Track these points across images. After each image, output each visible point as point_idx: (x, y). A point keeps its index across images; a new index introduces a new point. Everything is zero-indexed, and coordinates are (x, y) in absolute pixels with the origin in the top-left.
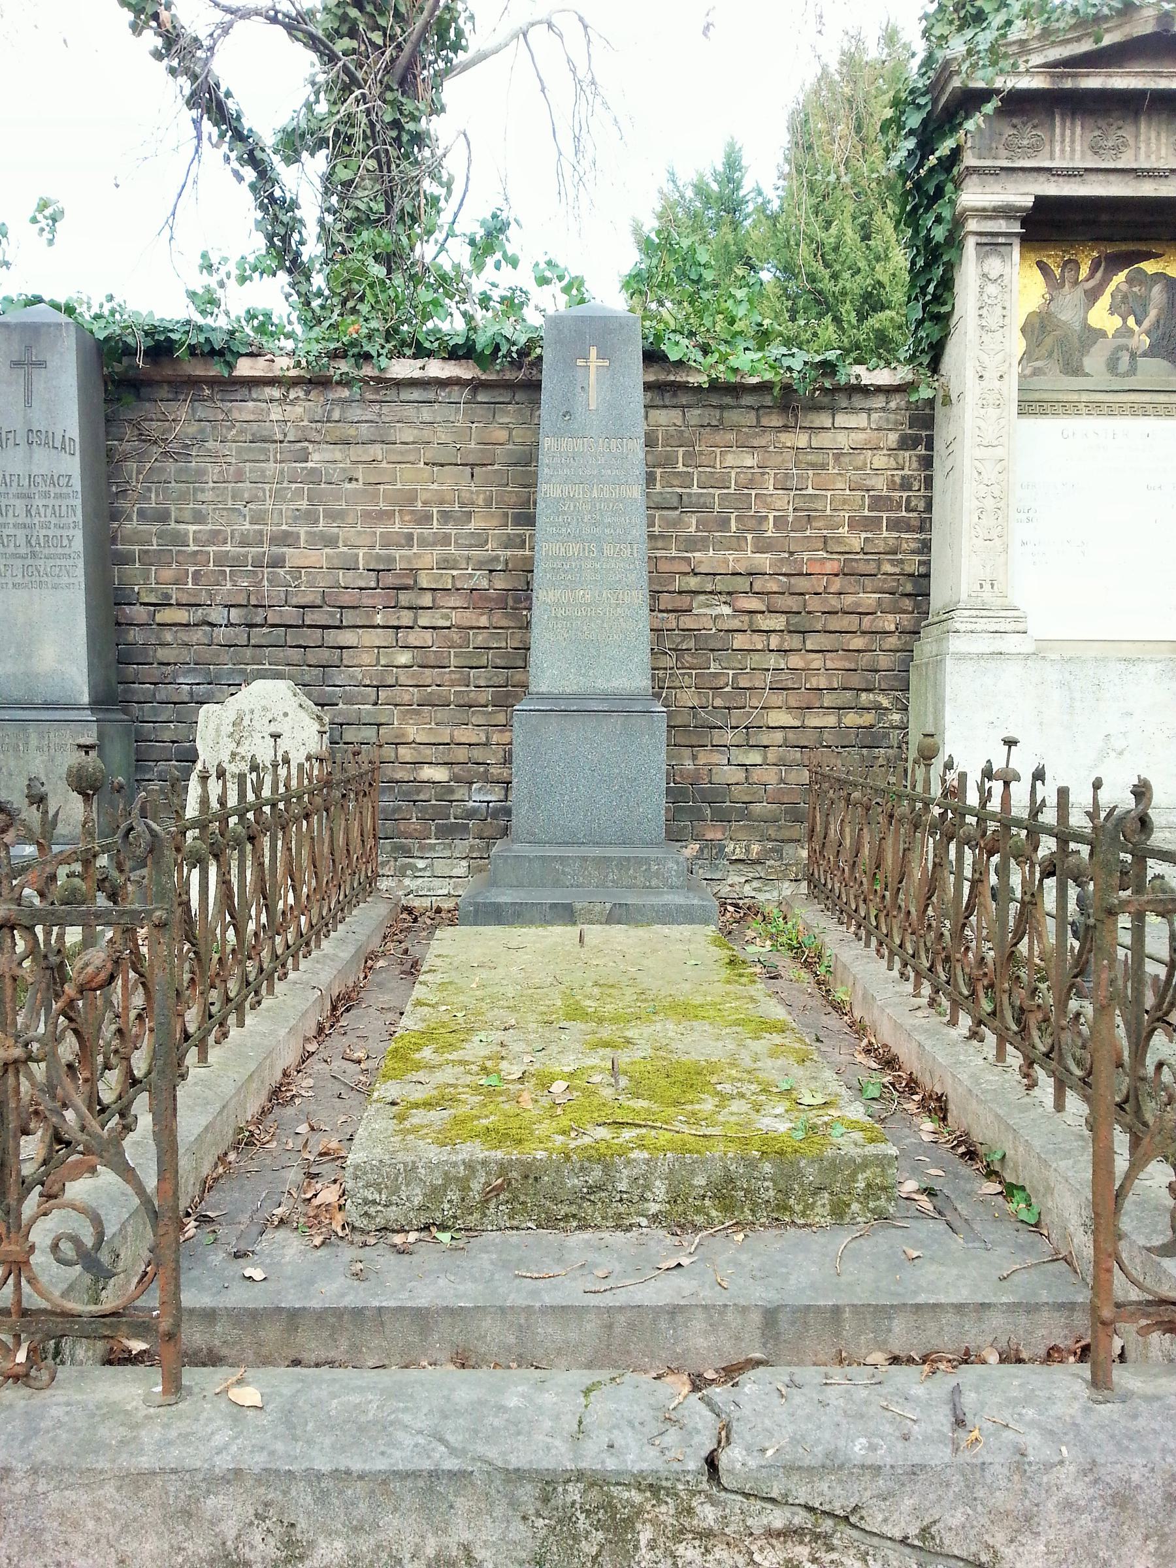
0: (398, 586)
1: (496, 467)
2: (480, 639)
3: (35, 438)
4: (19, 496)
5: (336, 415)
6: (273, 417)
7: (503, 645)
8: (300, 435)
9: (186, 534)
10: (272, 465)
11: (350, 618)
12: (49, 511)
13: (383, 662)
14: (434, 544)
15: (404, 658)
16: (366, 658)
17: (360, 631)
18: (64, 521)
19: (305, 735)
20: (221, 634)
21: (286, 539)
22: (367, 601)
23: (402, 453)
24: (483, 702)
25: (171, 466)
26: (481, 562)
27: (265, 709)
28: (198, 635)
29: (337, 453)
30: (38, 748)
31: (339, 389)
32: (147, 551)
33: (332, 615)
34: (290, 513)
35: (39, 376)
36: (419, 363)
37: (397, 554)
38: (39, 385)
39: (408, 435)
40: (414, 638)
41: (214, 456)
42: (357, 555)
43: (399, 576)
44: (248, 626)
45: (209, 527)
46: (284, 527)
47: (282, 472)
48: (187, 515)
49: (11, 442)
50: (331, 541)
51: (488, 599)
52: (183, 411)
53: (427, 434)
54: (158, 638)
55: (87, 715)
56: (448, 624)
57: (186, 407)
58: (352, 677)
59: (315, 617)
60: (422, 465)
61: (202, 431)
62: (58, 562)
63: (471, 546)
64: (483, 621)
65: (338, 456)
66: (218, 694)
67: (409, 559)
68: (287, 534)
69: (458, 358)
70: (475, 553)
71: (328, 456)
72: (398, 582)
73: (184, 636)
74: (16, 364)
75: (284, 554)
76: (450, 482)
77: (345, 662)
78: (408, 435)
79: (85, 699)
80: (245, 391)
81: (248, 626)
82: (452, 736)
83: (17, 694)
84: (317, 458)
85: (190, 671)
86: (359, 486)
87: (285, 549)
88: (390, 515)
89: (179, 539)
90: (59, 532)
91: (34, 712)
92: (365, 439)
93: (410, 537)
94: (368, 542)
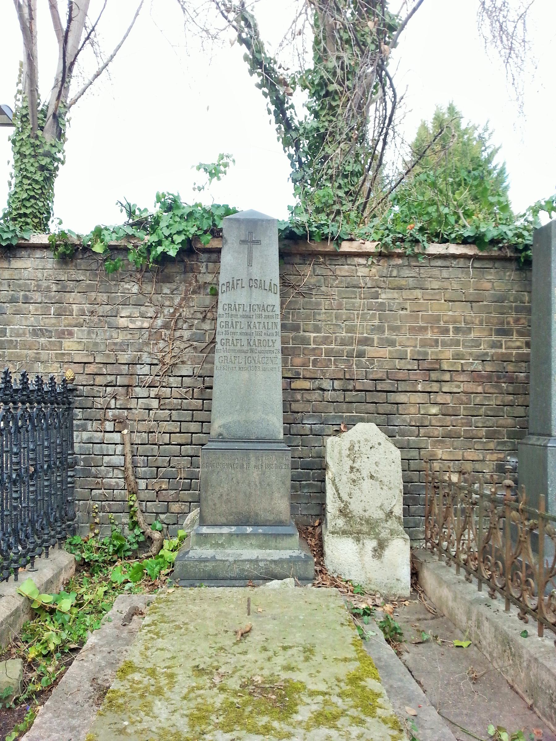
0: (431, 369)
1: (485, 303)
2: (478, 400)
3: (254, 284)
4: (243, 317)
5: (395, 273)
6: (359, 274)
7: (491, 403)
8: (374, 284)
9: (310, 338)
10: (358, 300)
11: (402, 386)
12: (262, 325)
13: (422, 412)
14: (451, 345)
15: (434, 410)
16: (413, 410)
17: (408, 394)
18: (270, 331)
19: (393, 456)
20: (329, 395)
21: (366, 342)
22: (413, 377)
23: (432, 295)
24: (480, 436)
25: (301, 300)
26: (478, 356)
27: (366, 440)
28: (316, 395)
29: (395, 294)
30: (255, 467)
31: (397, 259)
32: (287, 348)
33: (393, 385)
34: (368, 327)
35: (256, 249)
36: (444, 246)
37: (429, 351)
38: (256, 253)
39: (436, 285)
40: (440, 398)
41: (326, 295)
42: (407, 351)
43: (431, 363)
44: (344, 391)
45: (322, 334)
46: (365, 335)
47: (364, 304)
48: (310, 327)
49: (239, 285)
50: (392, 343)
51: (482, 377)
52: (308, 270)
53: (446, 284)
54: (292, 397)
55: (283, 446)
56: (459, 391)
57: (311, 268)
58: (404, 421)
59: (383, 386)
60: (443, 301)
61: (319, 281)
62: (266, 355)
63: (472, 346)
64: (480, 389)
65: (396, 296)
66: (327, 430)
67: (436, 353)
68: (367, 339)
69: (470, 243)
70: (474, 350)
71: (390, 296)
72: (430, 367)
73: (307, 396)
74: (243, 242)
75: (365, 350)
76: (459, 311)
77: (400, 412)
78: (436, 285)
79: (281, 436)
80: (343, 259)
81: (344, 391)
82: (463, 456)
83: (240, 434)
84: (384, 296)
85: (310, 416)
86: (408, 312)
87: (365, 347)
88: (425, 329)
89: (305, 341)
90: (267, 338)
91: (251, 444)
92: (411, 286)
93: (437, 341)
94: (413, 344)
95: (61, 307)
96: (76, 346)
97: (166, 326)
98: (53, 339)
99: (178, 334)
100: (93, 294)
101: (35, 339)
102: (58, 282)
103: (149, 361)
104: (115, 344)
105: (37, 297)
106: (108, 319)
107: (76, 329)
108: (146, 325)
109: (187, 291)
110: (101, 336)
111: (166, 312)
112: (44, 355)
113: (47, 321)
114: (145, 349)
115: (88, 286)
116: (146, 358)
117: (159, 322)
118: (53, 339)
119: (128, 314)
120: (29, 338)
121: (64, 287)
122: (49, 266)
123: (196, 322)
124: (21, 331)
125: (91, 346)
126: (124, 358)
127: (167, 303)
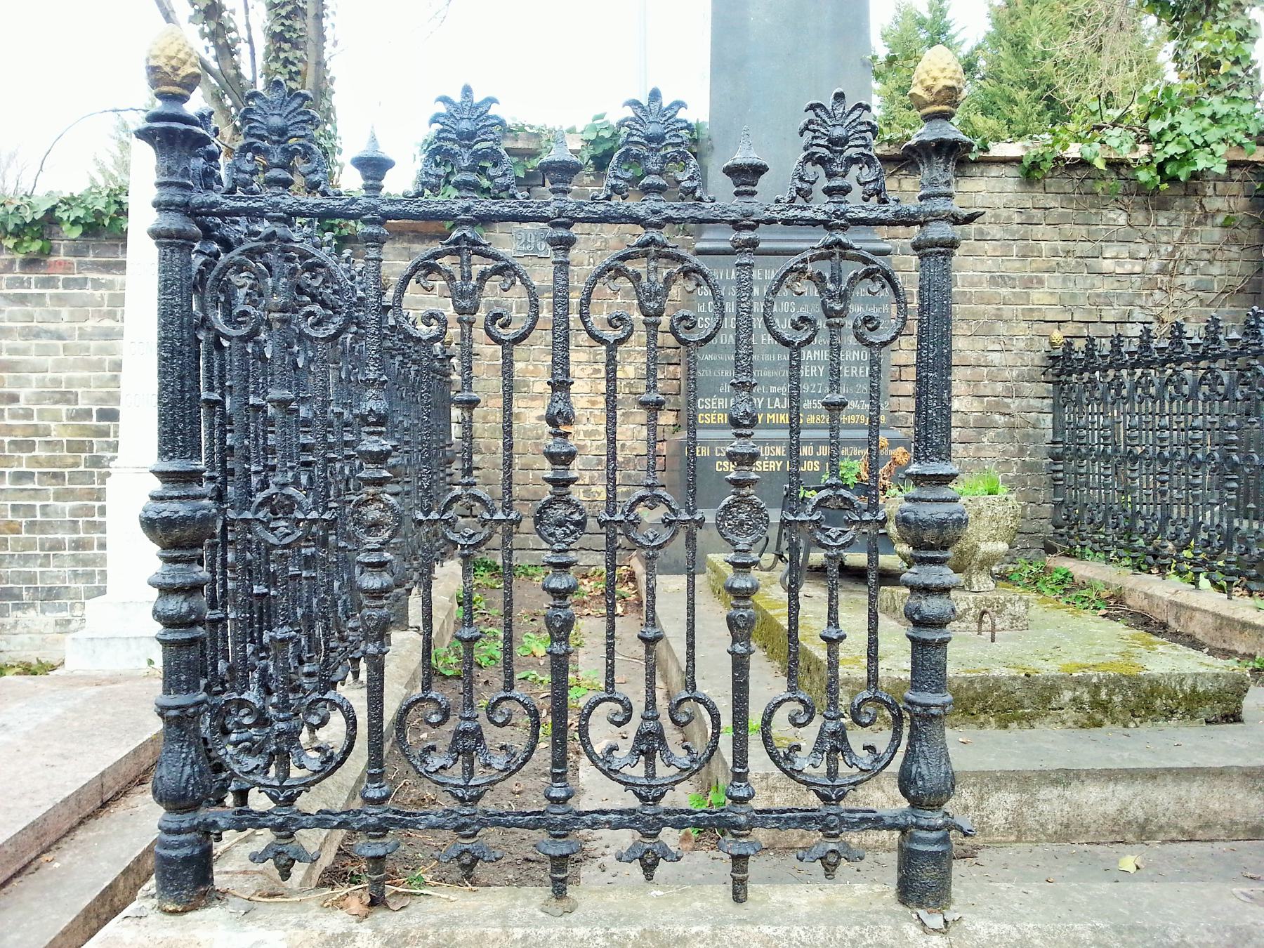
95: (1027, 245)
96: (1048, 300)
97: (1163, 271)
98: (1017, 290)
99: (1179, 280)
100: (1067, 226)
101: (994, 289)
102: (1021, 210)
103: (1142, 318)
104: (1099, 295)
105: (995, 231)
106: (1089, 261)
107: (1046, 275)
108: (1138, 269)
109: (1188, 222)
110: (1081, 284)
111: (1162, 250)
112: (1007, 311)
113: (1009, 265)
114: (1138, 302)
115: (1061, 215)
116: (1138, 315)
117: (1155, 265)
118: (1017, 290)
119: (1114, 254)
120: (986, 288)
121: (1030, 217)
122: (1010, 188)
123: (1202, 264)
124: (976, 279)
125: (1067, 297)
126: (1110, 314)
127: (1164, 239)
